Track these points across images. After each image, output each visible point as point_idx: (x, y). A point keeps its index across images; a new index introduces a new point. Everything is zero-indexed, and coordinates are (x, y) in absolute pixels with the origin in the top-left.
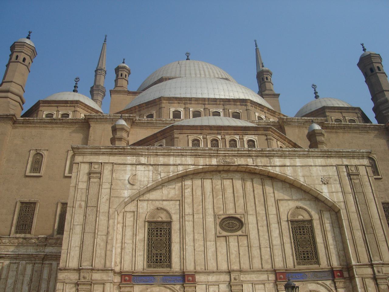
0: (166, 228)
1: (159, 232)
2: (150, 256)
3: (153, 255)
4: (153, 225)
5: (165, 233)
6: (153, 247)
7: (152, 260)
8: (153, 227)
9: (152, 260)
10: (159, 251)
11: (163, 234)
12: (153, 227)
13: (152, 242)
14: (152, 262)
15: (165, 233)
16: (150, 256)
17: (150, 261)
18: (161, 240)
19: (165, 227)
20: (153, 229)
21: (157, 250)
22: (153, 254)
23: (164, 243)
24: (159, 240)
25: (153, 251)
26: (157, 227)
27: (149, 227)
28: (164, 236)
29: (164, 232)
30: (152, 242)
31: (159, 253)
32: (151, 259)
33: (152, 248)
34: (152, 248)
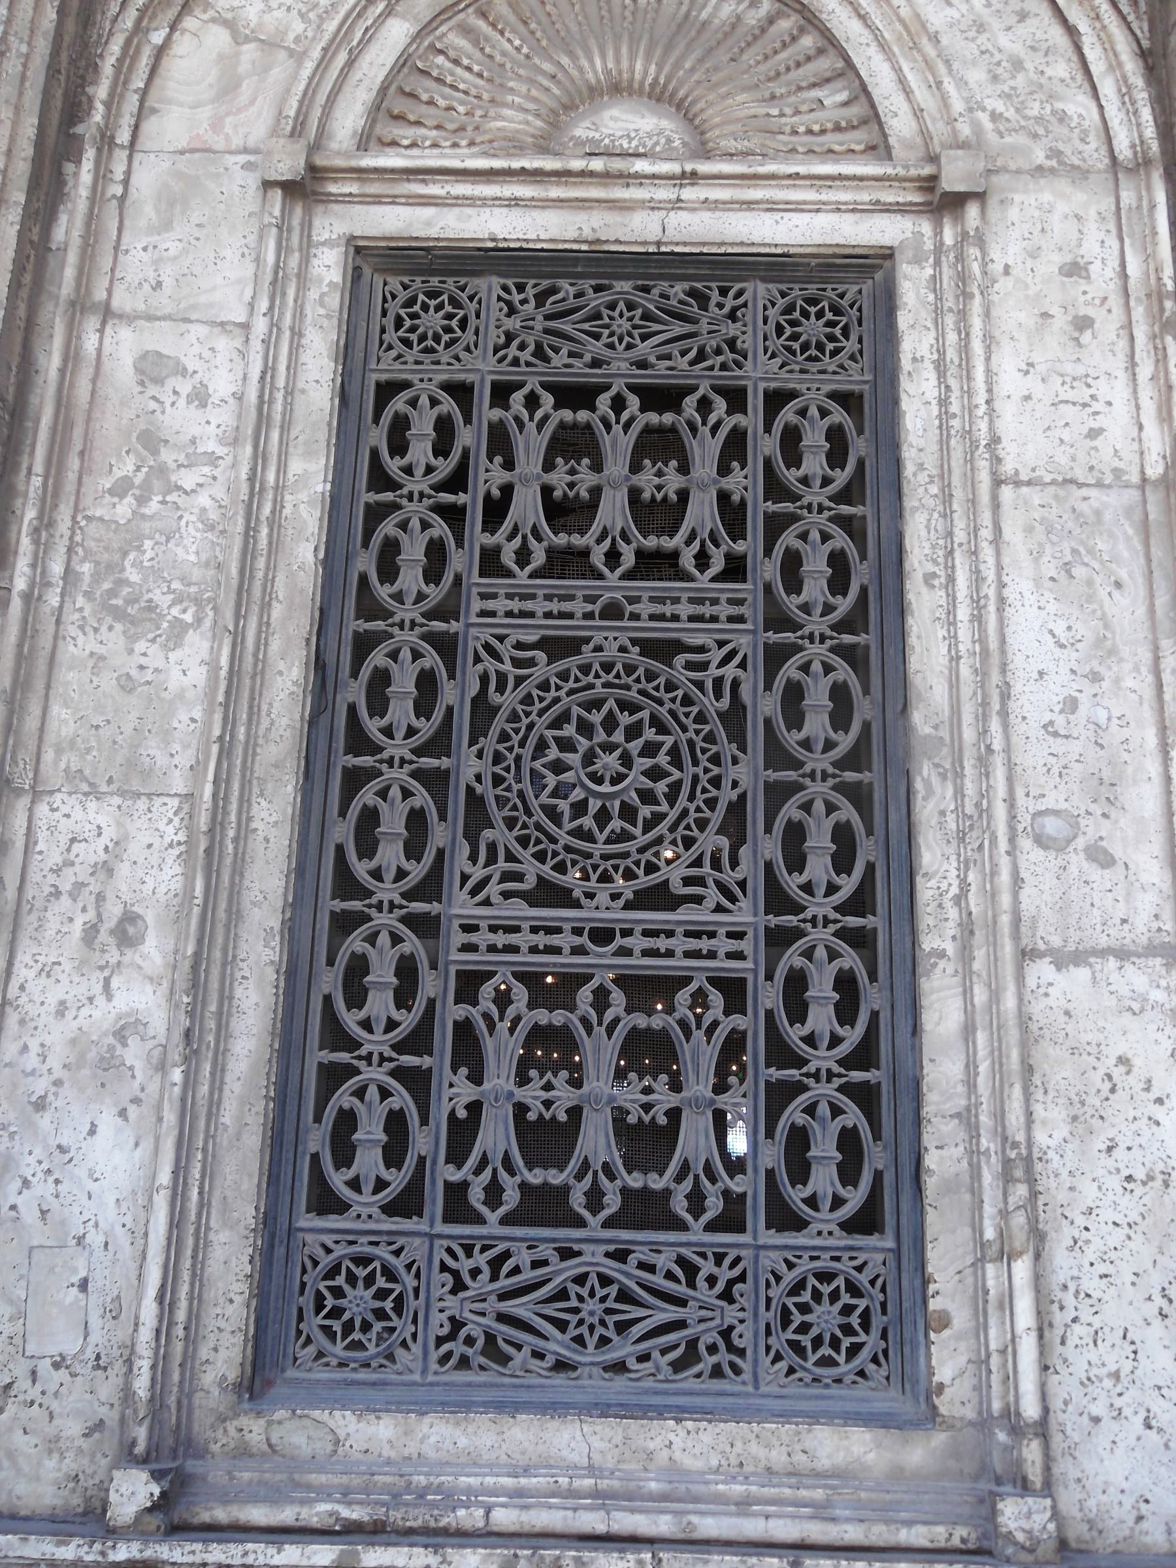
0: (776, 400)
1: (617, 466)
2: (377, 1042)
4: (494, 322)
5: (759, 508)
6: (474, 801)
7: (425, 1141)
8: (482, 369)
10: (603, 909)
11: (702, 513)
12: (482, 369)
14: (407, 1204)
15: (759, 508)
16: (377, 1042)
17: (369, 1160)
18: (663, 650)
19: (760, 374)
21: (550, 894)
22: (469, 984)
23: (735, 718)
24: (611, 640)
25: (459, 905)
27: (386, 368)
28: (735, 569)
29: (735, 482)
31: (602, 958)
32: (396, 1123)
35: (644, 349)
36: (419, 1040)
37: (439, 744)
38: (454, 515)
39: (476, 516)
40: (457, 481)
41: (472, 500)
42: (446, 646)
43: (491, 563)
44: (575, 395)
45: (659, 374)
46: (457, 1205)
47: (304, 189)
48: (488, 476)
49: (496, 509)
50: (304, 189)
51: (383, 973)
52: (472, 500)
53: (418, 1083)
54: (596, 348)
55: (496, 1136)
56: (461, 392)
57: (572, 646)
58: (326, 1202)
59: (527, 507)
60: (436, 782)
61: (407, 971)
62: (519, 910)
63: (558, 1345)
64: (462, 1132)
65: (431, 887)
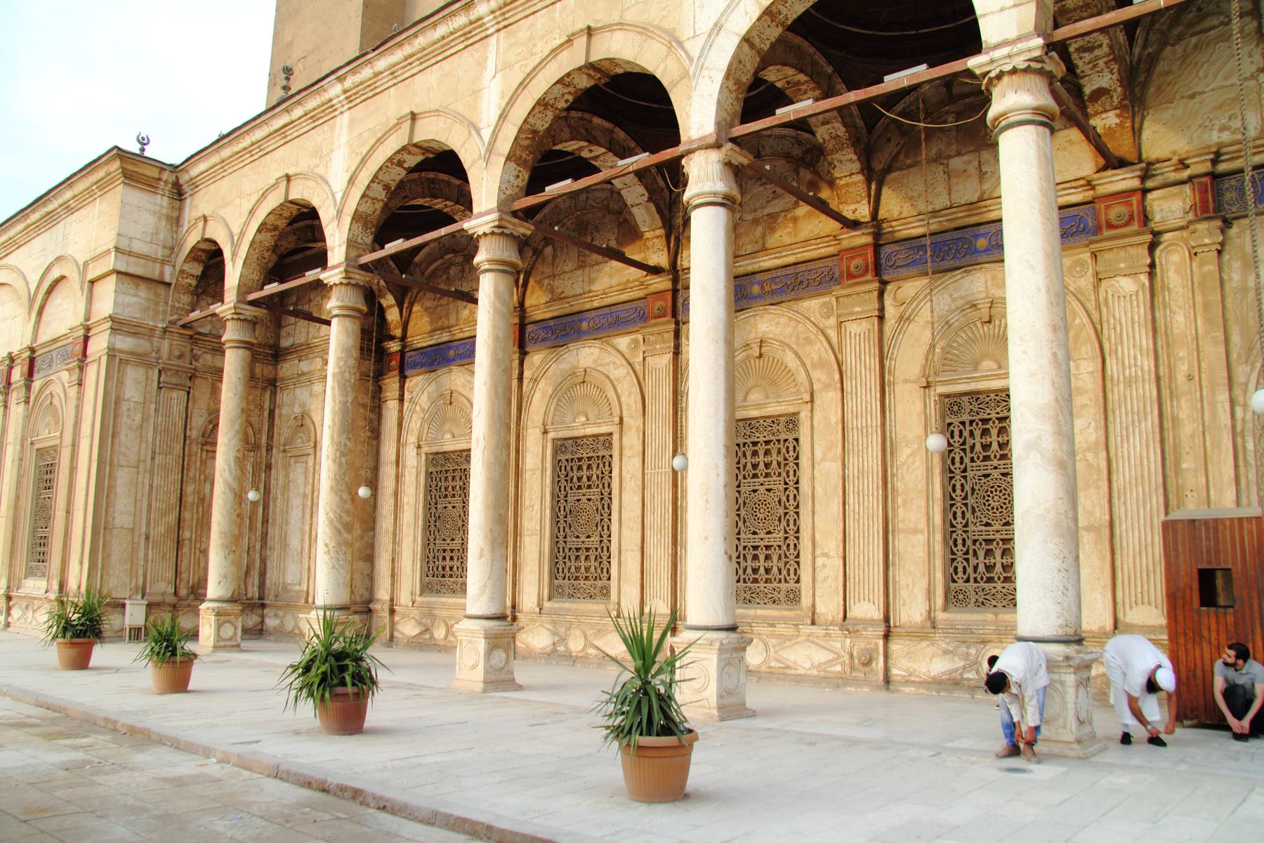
3: (972, 548)
7: (970, 570)
8: (966, 418)
9: (970, 570)
13: (967, 488)
14: (967, 581)
17: (960, 574)
20: (968, 428)
21: (987, 524)
26: (986, 416)
27: (948, 420)
30: (967, 488)
33: (968, 515)
34: (968, 515)
35: (998, 410)
36: (967, 553)
37: (965, 498)
38: (964, 450)
39: (968, 451)
40: (964, 443)
41: (967, 447)
42: (965, 477)
43: (972, 460)
44: (985, 421)
45: (1001, 415)
46: (976, 581)
47: (928, 386)
48: (970, 441)
49: (972, 448)
50: (928, 386)
51: (960, 541)
52: (967, 447)
53: (967, 560)
54: (988, 411)
55: (981, 568)
56: (963, 423)
57: (988, 476)
58: (954, 581)
59: (978, 448)
60: (966, 505)
61: (964, 540)
62: (983, 528)
63: (994, 603)
64: (976, 568)
65: (966, 525)
